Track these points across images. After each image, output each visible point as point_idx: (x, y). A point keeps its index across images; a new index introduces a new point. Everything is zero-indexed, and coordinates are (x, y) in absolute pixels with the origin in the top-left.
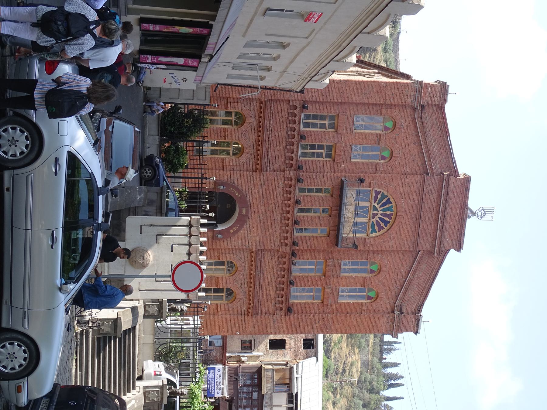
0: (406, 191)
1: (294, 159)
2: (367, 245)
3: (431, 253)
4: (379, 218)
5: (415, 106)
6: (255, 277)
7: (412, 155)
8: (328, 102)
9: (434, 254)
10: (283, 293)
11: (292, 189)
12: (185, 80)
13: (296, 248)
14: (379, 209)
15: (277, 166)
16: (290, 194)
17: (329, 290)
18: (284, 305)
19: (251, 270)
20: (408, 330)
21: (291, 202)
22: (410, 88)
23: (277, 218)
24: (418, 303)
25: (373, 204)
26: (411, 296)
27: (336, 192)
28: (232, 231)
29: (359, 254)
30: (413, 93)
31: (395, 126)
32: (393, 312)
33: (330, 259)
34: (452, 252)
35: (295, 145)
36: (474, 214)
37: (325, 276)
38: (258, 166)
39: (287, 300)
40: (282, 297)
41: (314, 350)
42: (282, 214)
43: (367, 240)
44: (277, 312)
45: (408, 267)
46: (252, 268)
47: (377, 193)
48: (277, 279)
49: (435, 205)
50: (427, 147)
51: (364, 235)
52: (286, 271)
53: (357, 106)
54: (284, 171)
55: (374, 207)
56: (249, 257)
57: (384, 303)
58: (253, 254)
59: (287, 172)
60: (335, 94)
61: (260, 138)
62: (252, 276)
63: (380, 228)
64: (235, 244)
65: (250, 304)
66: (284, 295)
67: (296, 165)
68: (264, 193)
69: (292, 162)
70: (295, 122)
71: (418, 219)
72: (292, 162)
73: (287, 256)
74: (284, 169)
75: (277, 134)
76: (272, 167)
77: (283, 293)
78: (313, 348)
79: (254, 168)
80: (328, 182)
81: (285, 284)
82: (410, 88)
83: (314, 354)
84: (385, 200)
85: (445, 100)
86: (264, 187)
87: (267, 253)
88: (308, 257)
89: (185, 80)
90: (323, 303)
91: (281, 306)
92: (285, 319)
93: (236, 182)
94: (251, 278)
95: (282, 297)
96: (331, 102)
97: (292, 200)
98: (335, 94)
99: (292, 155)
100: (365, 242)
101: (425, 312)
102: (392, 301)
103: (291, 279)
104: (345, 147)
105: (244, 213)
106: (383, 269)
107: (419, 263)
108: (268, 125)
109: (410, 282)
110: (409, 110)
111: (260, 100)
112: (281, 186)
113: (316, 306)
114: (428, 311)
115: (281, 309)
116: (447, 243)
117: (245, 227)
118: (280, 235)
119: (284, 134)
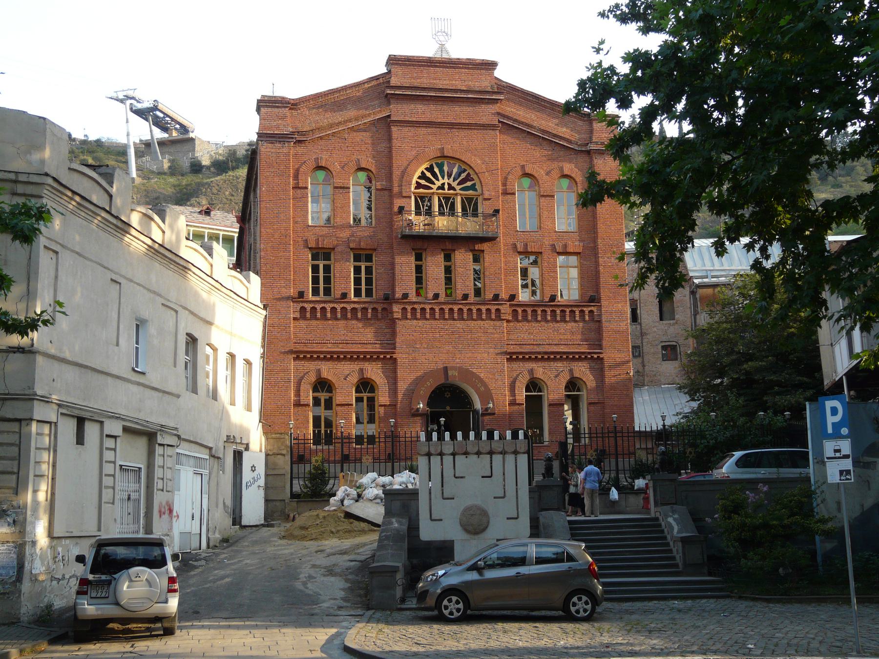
1: (375, 306)
6: (546, 353)
12: (253, 468)
14: (441, 181)
34: (498, 73)
35: (356, 306)
36: (442, 47)
47: (419, 185)
55: (439, 188)
62: (546, 357)
69: (380, 309)
71: (451, 126)
72: (380, 309)
79: (391, 362)
82: (268, 150)
89: (253, 468)
91: (587, 312)
117: (474, 371)
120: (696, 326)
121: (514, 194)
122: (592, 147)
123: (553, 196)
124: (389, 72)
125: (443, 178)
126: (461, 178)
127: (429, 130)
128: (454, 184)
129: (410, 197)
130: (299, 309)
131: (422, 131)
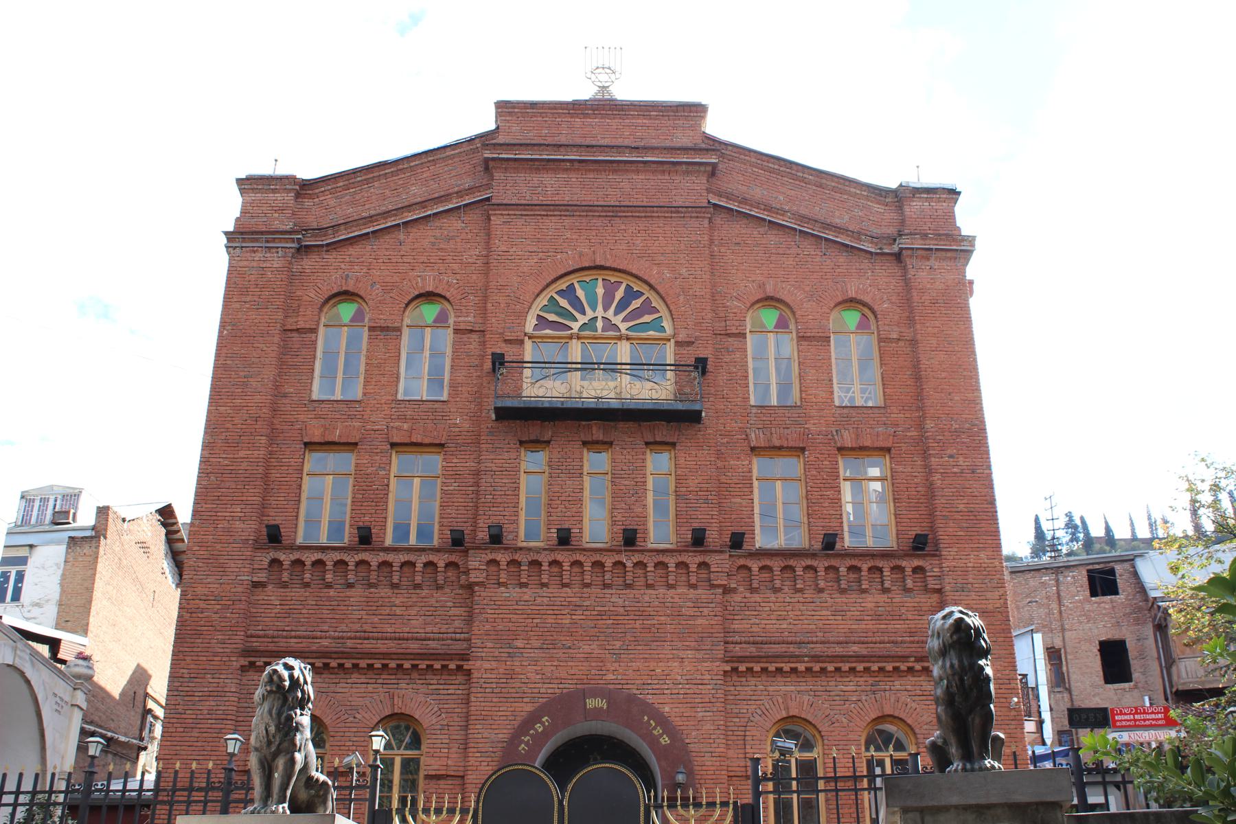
0: (535, 249)
1: (432, 558)
2: (697, 338)
3: (713, 171)
4: (616, 313)
5: (295, 245)
6: (816, 658)
7: (433, 244)
8: (266, 476)
9: (714, 166)
10: (865, 567)
11: (523, 558)
13: (712, 537)
14: (590, 314)
15: (454, 611)
16: (540, 564)
17: (846, 434)
18: (904, 564)
19: (794, 670)
20: (951, 216)
21: (564, 557)
22: (246, 263)
23: (617, 599)
25: (575, 330)
26: (846, 217)
27: (534, 430)
28: (665, 740)
29: (727, 358)
30: (258, 256)
31: (346, 295)
32: (898, 257)
33: (747, 438)
35: (390, 557)
37: (803, 449)
38: (452, 666)
39: (885, 555)
40: (880, 570)
41: (1118, 568)
42: (606, 586)
43: (682, 337)
44: (932, 583)
45: (762, 230)
46: (786, 667)
48: (821, 591)
49: (574, 177)
50: (409, 207)
51: (670, 349)
52: (792, 562)
53: (285, 396)
54: (470, 587)
56: (753, 681)
57: (876, 283)
58: (742, 668)
59: (473, 577)
60: (242, 454)
61: (363, 663)
62: (817, 667)
63: (647, 308)
64: (708, 726)
65: (910, 669)
66: (870, 563)
67: (451, 552)
68: (537, 644)
69: (441, 564)
70: (319, 563)
71: (614, 212)
72: (441, 564)
73: (742, 562)
74: (462, 587)
75: (357, 615)
76: (457, 624)
77: (865, 567)
78: (1112, 572)
79: (460, 678)
80: (506, 456)
81: (834, 562)
82: (246, 263)
83: (1127, 565)
84: (563, 303)
85: (291, 179)
86: (519, 643)
87: (736, 626)
88: (744, 503)
90: (889, 450)
91: (909, 570)
92: (951, 556)
93: (504, 735)
94: (823, 670)
95: (880, 570)
96: (268, 468)
97: (559, 557)
98: (242, 454)
99: (419, 566)
100: (690, 343)
101: (890, 182)
102: (866, 264)
103: (818, 546)
104: (404, 419)
105: (601, 703)
106: (770, 290)
107: (744, 201)
108: (325, 643)
109: (803, 218)
110: (308, 263)
111: (243, 669)
112: (515, 592)
113: (900, 469)
115: (917, 570)
116: (683, 140)
117: (650, 699)
118: (670, 587)
119: (357, 593)
120: (1171, 686)
121: (744, 335)
122: (905, 242)
124: (498, 128)
126: (629, 309)
127: (567, 222)
128: (617, 320)
129: (522, 342)
130: (266, 563)
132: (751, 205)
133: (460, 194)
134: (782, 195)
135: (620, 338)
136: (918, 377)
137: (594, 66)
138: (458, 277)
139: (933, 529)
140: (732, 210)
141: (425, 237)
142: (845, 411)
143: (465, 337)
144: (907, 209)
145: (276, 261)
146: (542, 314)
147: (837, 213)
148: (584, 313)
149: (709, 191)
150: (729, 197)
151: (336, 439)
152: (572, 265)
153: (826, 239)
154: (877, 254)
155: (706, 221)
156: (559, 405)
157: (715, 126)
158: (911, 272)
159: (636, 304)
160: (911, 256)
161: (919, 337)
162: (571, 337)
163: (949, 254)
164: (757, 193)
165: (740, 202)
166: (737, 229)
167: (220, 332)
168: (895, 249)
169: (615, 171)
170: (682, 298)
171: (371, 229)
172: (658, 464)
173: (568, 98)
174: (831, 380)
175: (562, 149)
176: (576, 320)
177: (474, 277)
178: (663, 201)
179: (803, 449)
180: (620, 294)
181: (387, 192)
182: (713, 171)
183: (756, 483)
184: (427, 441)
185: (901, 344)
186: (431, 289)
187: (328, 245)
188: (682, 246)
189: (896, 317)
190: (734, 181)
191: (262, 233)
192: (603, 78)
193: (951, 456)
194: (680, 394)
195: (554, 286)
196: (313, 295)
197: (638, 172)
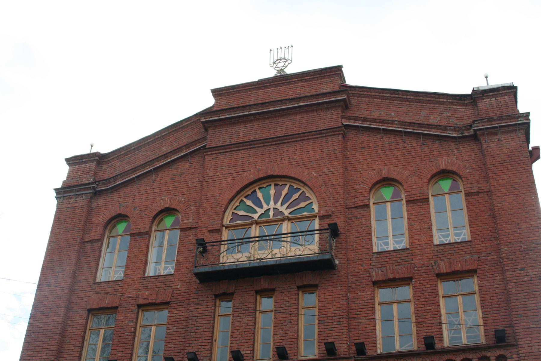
4: (282, 205)
14: (265, 207)
17: (441, 263)
18: (489, 354)
24: (452, 103)
26: (438, 118)
27: (223, 288)
32: (475, 137)
33: (370, 276)
37: (411, 279)
49: (257, 125)
51: (317, 221)
60: (50, 319)
63: (303, 197)
66: (462, 356)
82: (65, 206)
84: (249, 203)
85: (97, 154)
102: (453, 145)
104: (146, 288)
106: (385, 173)
107: (365, 120)
110: (100, 201)
114: (460, 82)
122: (478, 126)
123: (427, 200)
125: (268, 205)
127: (251, 152)
128: (283, 209)
131: (242, 154)
132: (371, 121)
133: (187, 146)
134: (394, 113)
135: (283, 220)
136: (494, 217)
137: (275, 59)
138: (185, 196)
139: (511, 326)
140: (357, 127)
141: (166, 176)
142: (441, 248)
143: (187, 233)
144: (479, 105)
145: (82, 202)
146: (235, 211)
147: (432, 117)
148: (261, 207)
149: (342, 117)
150: (356, 119)
151: (106, 305)
152: (253, 178)
153: (424, 134)
154: (459, 138)
155: (340, 137)
156: (235, 267)
157: (352, 79)
158: (485, 145)
159: (295, 196)
160: (484, 135)
161: (492, 188)
162: (251, 224)
163: (511, 128)
164: (377, 114)
165: (363, 121)
166: (364, 138)
167: (48, 247)
168: (472, 132)
169: (282, 116)
170: (323, 187)
171: (136, 175)
172: (309, 300)
173: (255, 78)
174: (430, 228)
175: (247, 108)
176: (256, 212)
177: (195, 195)
178: (313, 128)
179: (411, 279)
180: (295, 196)
181: (149, 153)
182: (345, 105)
183: (377, 307)
184: (158, 301)
185: (481, 195)
186: (167, 206)
187: (111, 188)
188: (325, 155)
189: (476, 178)
190: (362, 109)
191: (74, 186)
192: (281, 65)
193: (522, 269)
194: (322, 250)
195: (243, 193)
196: (101, 219)
197: (296, 114)
